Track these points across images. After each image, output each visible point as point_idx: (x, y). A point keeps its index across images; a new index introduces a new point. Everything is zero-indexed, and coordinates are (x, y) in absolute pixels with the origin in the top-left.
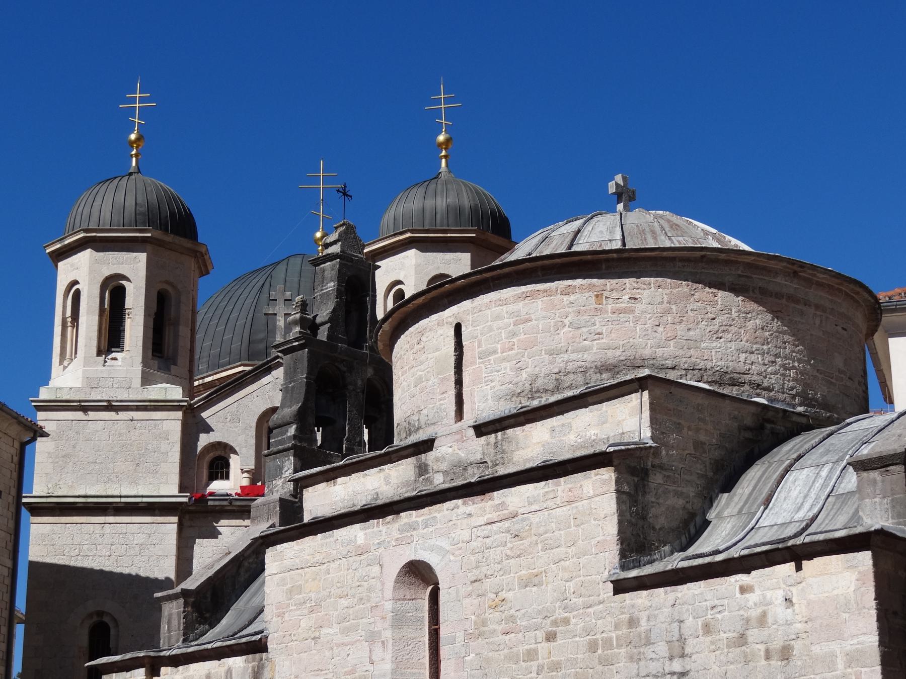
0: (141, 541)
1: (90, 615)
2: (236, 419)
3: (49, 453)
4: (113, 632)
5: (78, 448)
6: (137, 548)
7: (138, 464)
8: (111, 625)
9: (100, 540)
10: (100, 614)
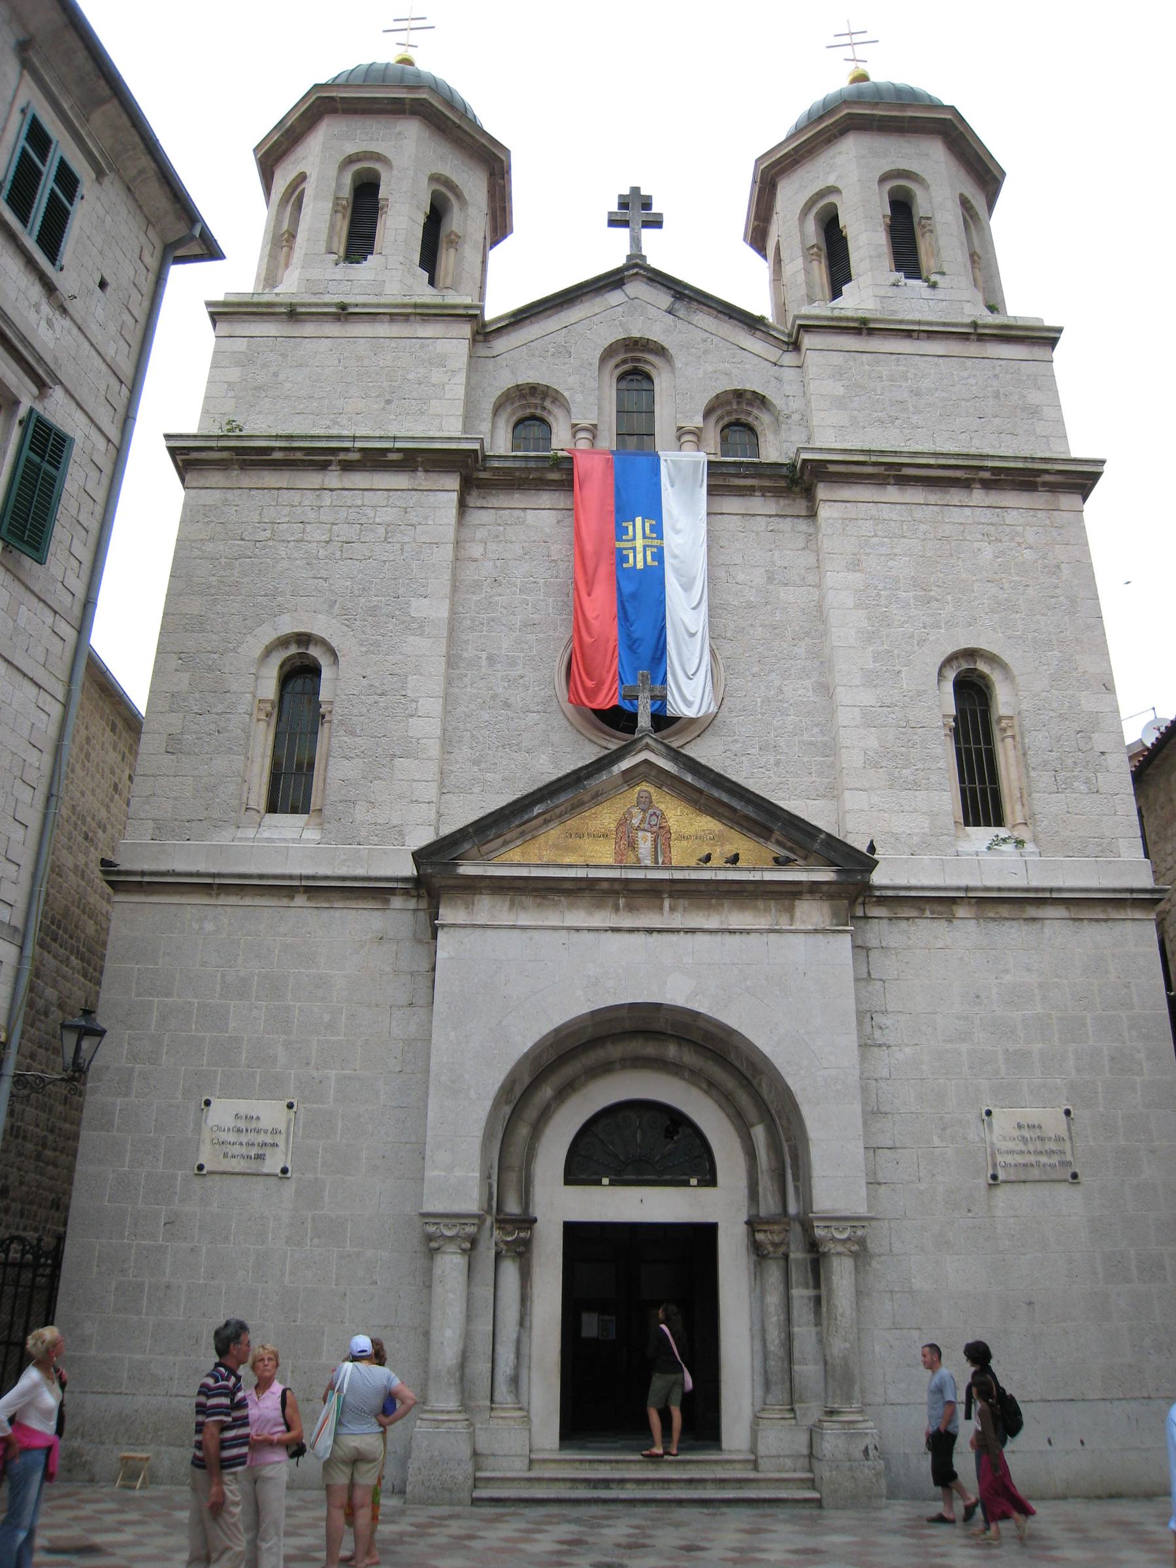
0: (388, 519)
1: (283, 642)
2: (564, 351)
3: (229, 383)
4: (326, 673)
5: (282, 377)
6: (381, 531)
7: (388, 402)
8: (324, 661)
9: (312, 516)
10: (304, 639)
